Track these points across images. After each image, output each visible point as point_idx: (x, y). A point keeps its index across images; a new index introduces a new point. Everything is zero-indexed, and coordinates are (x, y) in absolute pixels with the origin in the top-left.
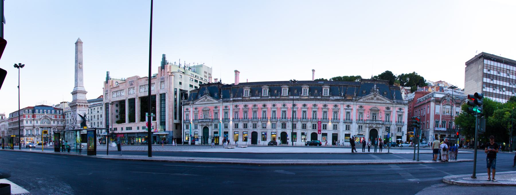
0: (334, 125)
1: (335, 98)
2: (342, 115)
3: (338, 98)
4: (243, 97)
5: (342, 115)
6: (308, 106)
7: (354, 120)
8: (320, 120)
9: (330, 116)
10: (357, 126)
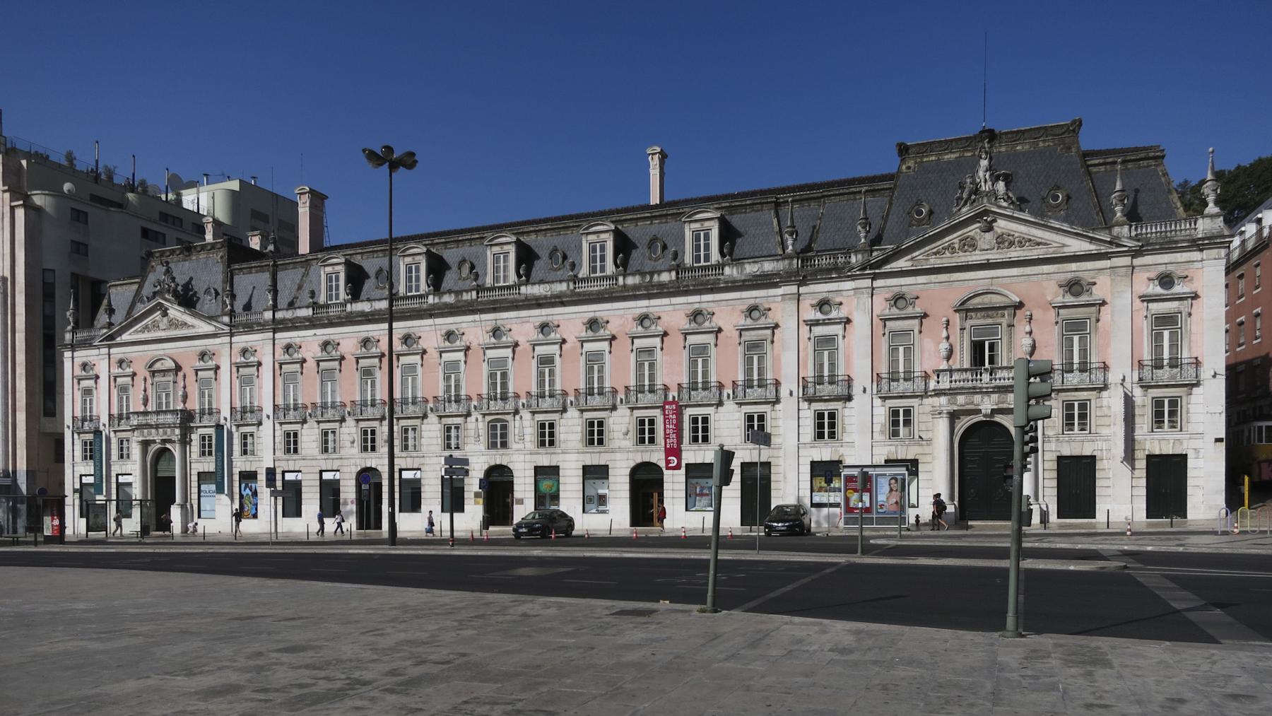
0: (750, 418)
1: (751, 268)
2: (788, 361)
3: (768, 266)
4: (315, 306)
5: (788, 361)
6: (612, 329)
7: (862, 378)
8: (673, 394)
9: (727, 365)
10: (882, 413)
